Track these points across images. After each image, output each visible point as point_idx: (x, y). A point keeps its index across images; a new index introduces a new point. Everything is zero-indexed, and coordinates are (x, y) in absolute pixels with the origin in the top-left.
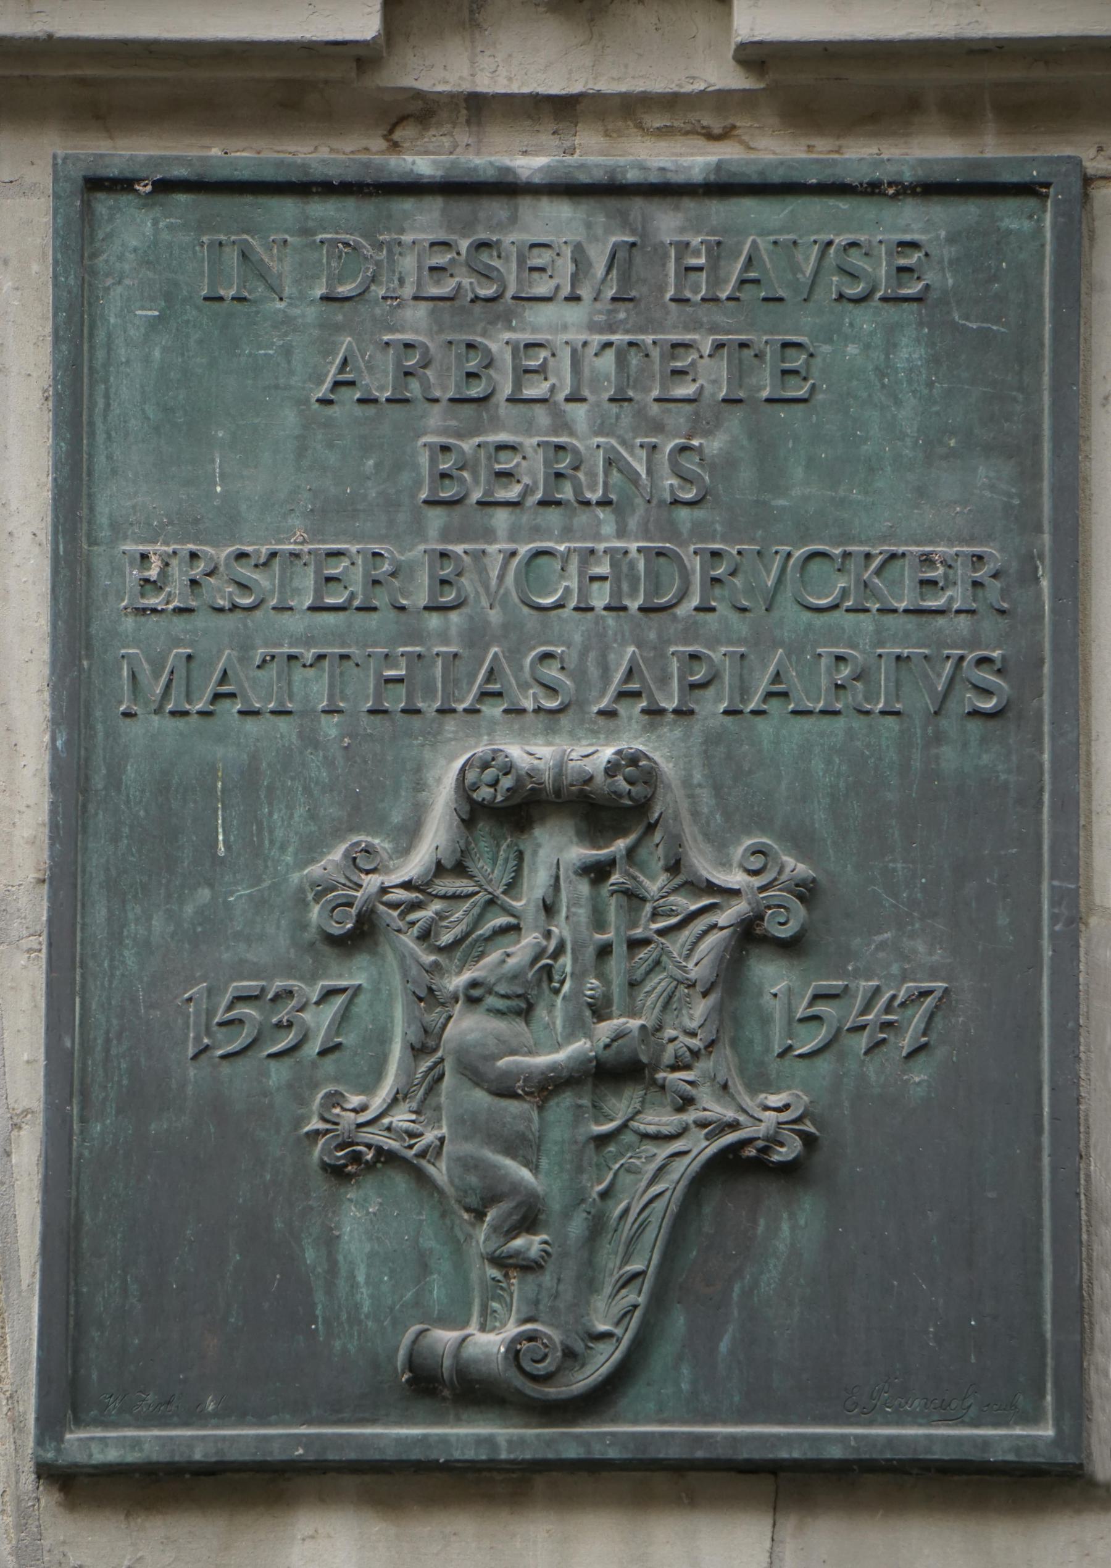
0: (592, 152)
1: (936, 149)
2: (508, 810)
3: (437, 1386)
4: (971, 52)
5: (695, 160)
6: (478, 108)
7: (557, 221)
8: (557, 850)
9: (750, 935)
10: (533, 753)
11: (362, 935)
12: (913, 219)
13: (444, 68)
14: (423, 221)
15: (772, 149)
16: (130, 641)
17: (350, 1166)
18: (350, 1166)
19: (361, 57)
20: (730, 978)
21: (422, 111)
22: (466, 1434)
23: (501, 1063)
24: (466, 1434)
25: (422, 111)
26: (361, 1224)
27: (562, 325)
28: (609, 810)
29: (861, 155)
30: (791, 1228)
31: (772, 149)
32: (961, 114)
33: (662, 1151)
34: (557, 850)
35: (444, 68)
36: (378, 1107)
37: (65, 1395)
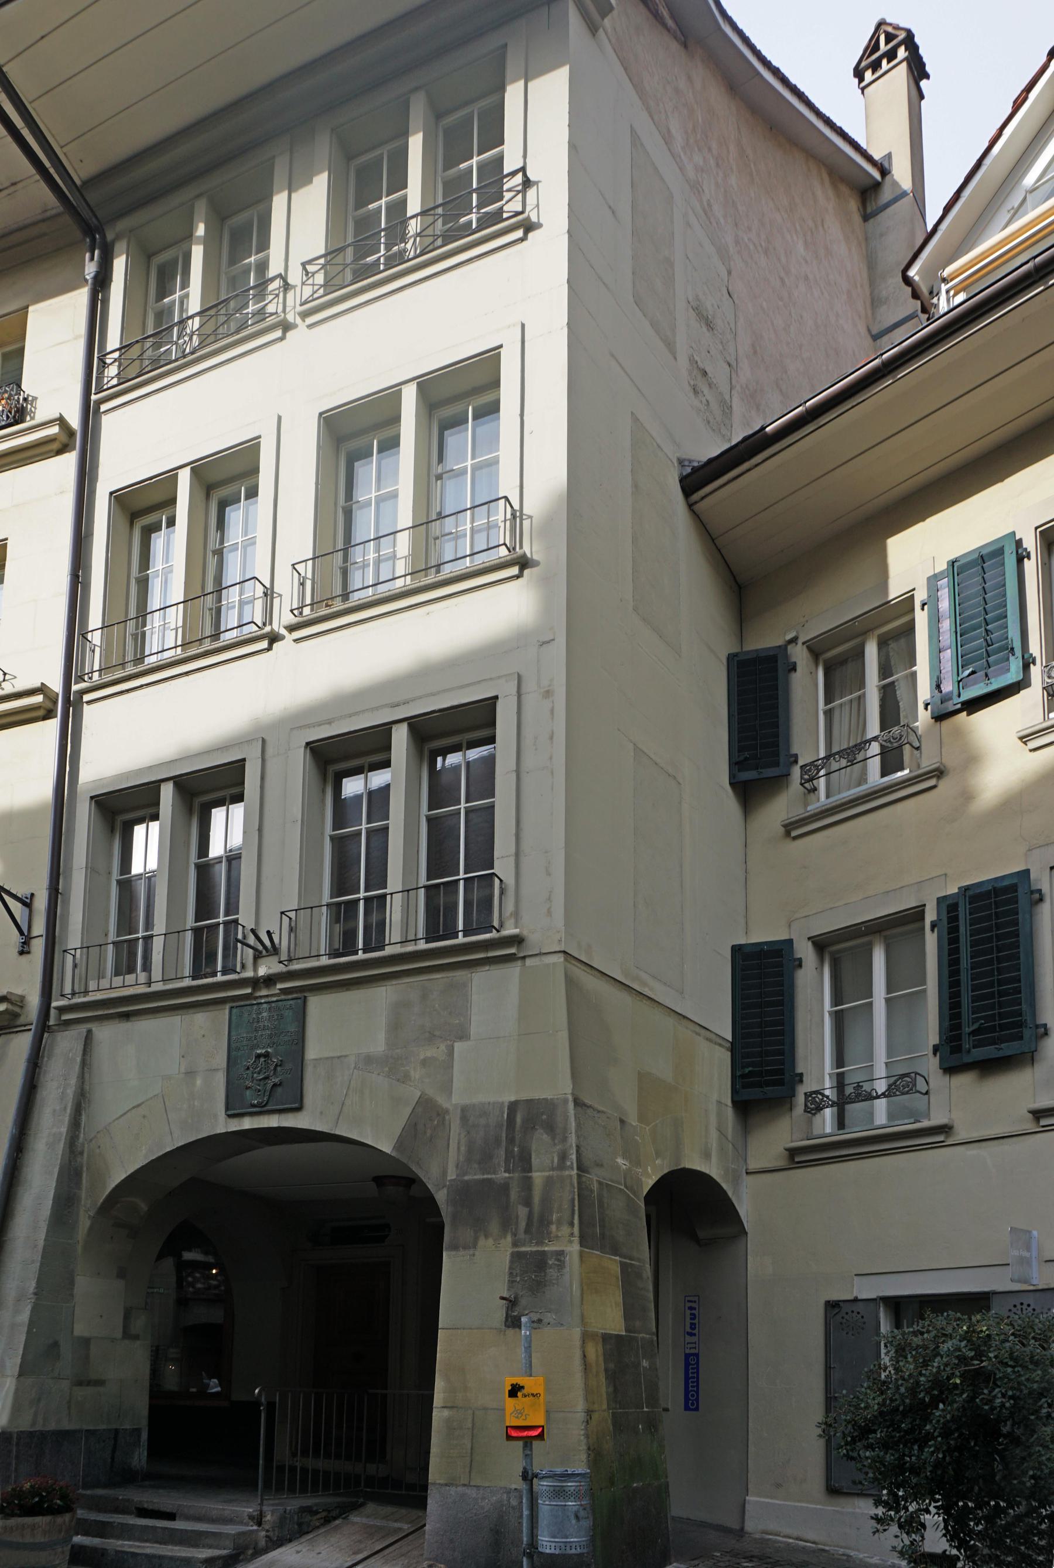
0: (267, 1000)
1: (295, 996)
2: (258, 1056)
3: (253, 1106)
4: (836, 995)
5: (275, 999)
6: (261, 997)
7: (265, 1006)
8: (262, 1059)
9: (276, 1065)
10: (259, 1051)
11: (248, 1068)
12: (291, 1002)
13: (258, 994)
14: (255, 1007)
15: (283, 997)
16: (233, 1046)
17: (247, 1088)
18: (247, 1088)
19: (251, 994)
20: (275, 1069)
21: (256, 998)
22: (254, 1110)
23: (768, 429)
24: (254, 1110)
25: (256, 998)
26: (248, 1092)
27: (265, 1014)
28: (266, 1055)
29: (290, 997)
30: (279, 1090)
31: (283, 997)
32: (296, 992)
33: (270, 1084)
34: (262, 1059)
35: (258, 994)
36: (249, 1083)
37: (227, 1109)
